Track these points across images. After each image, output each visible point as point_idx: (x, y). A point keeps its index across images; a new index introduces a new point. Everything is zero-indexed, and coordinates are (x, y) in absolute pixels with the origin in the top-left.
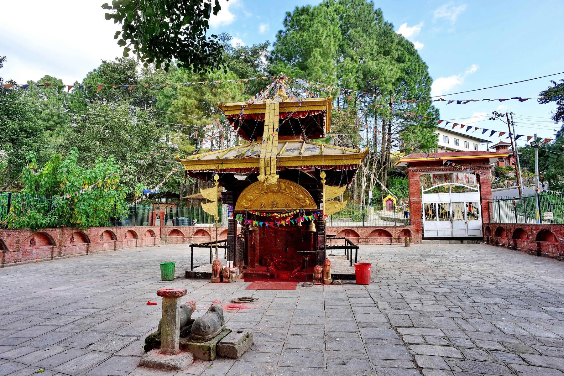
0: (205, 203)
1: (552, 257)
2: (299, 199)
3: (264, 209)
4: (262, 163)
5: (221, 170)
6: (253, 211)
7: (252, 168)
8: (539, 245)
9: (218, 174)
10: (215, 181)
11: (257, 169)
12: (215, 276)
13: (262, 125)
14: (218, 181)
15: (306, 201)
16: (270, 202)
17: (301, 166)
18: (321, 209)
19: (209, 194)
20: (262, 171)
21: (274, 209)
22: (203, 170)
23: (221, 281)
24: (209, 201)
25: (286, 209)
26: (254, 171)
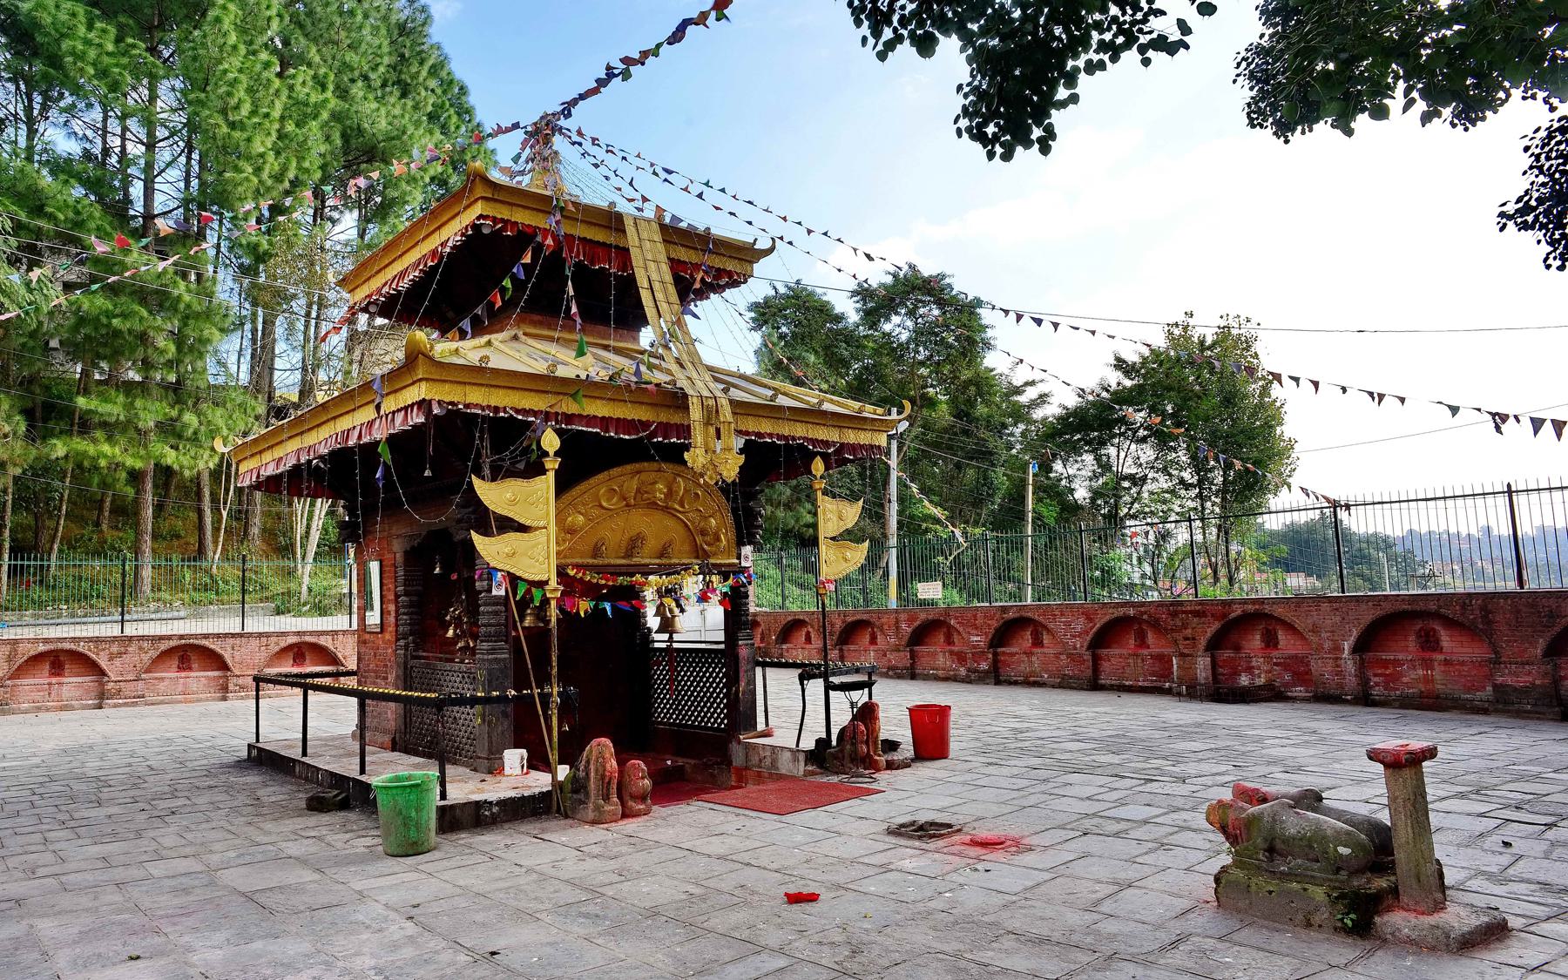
0: (486, 533)
1: (946, 679)
2: (703, 533)
3: (606, 561)
4: (696, 413)
5: (569, 418)
6: (578, 566)
7: (645, 425)
8: (913, 656)
9: (559, 432)
10: (546, 454)
11: (685, 431)
12: (607, 798)
13: (629, 286)
14: (557, 454)
15: (718, 539)
16: (627, 536)
17: (771, 436)
18: (744, 564)
19: (513, 502)
20: (698, 437)
21: (636, 560)
22: (496, 410)
23: (626, 815)
24: (523, 528)
25: (664, 561)
26: (654, 434)
